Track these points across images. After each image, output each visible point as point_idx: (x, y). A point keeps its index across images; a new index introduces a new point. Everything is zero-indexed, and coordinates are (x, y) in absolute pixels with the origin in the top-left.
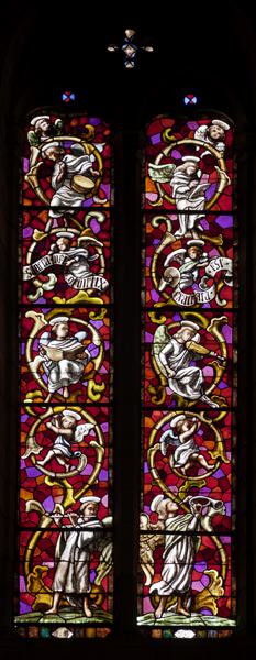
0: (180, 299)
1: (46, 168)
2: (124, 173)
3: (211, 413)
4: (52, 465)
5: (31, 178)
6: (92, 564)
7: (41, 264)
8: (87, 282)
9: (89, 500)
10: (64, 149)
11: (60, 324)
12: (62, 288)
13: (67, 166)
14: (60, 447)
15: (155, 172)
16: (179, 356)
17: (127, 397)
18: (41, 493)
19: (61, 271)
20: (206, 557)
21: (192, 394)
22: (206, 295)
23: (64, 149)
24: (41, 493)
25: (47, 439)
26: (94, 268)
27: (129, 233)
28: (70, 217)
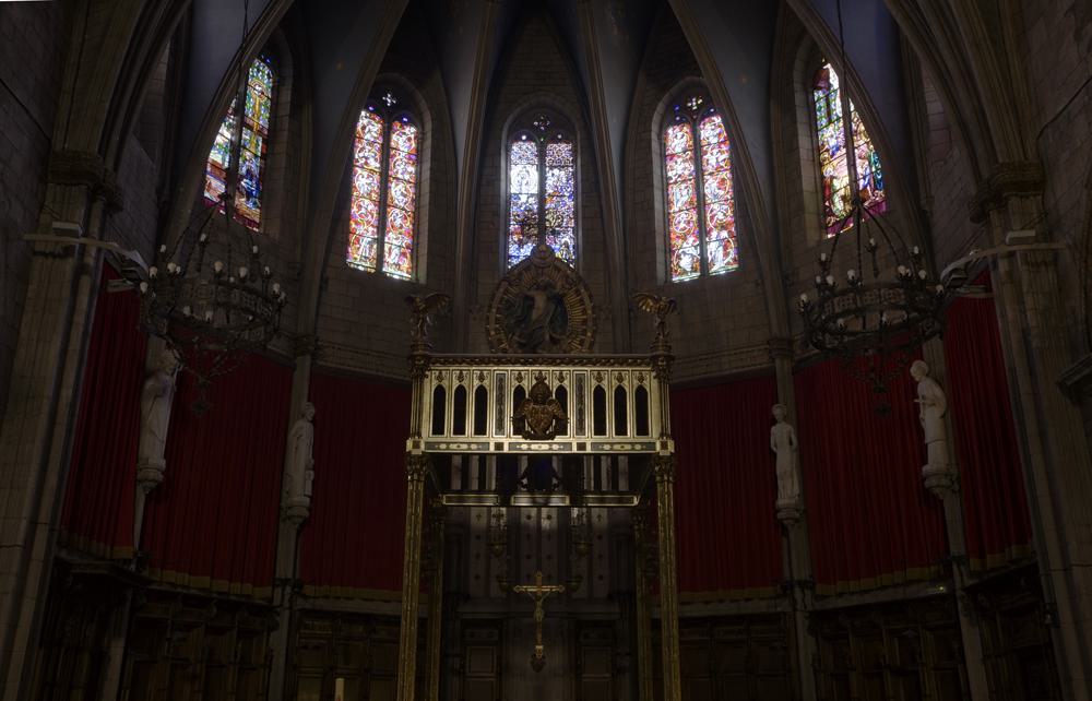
0: (400, 176)
1: (364, 128)
2: (386, 134)
3: (406, 211)
4: (360, 215)
5: (359, 128)
6: (371, 247)
7: (361, 155)
8: (374, 164)
9: (371, 229)
10: (369, 123)
11: (365, 174)
12: (366, 163)
13: (369, 127)
14: (363, 211)
15: (394, 137)
16: (399, 193)
17: (383, 203)
18: (357, 223)
19: (367, 158)
20: (404, 254)
21: (402, 205)
22: (407, 177)
23: (369, 123)
24: (357, 223)
25: (360, 207)
26: (376, 160)
27: (386, 152)
28: (371, 144)
